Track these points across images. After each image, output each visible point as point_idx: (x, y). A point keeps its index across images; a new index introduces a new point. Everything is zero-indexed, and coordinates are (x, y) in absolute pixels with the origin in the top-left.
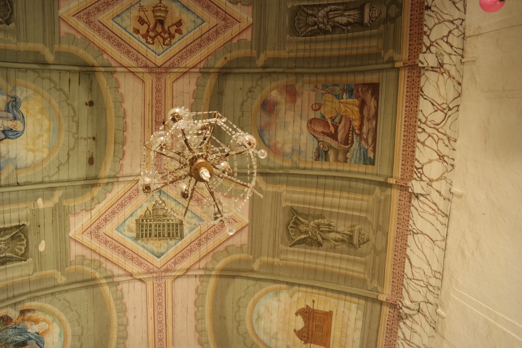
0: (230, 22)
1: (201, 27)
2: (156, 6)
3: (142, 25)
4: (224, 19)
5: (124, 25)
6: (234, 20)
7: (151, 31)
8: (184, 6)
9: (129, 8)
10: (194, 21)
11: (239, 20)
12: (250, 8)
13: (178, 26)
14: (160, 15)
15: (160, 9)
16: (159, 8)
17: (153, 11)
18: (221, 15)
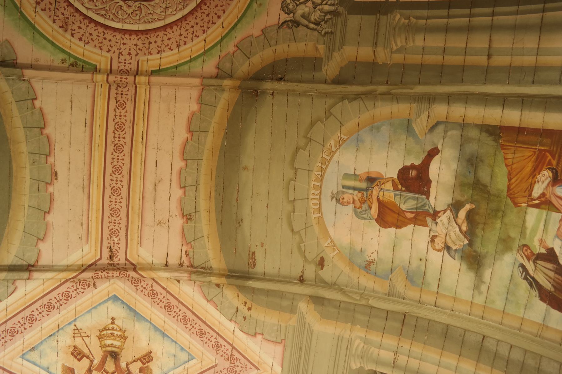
0: (240, 365)
1: (186, 365)
2: (105, 329)
3: (79, 360)
4: (230, 359)
5: (45, 363)
6: (247, 363)
7: (96, 369)
8: (156, 329)
9: (54, 333)
10: (175, 356)
11: (257, 365)
12: (279, 348)
13: (145, 361)
14: (112, 344)
15: (112, 334)
16: (110, 332)
17: (99, 337)
18: (225, 350)
